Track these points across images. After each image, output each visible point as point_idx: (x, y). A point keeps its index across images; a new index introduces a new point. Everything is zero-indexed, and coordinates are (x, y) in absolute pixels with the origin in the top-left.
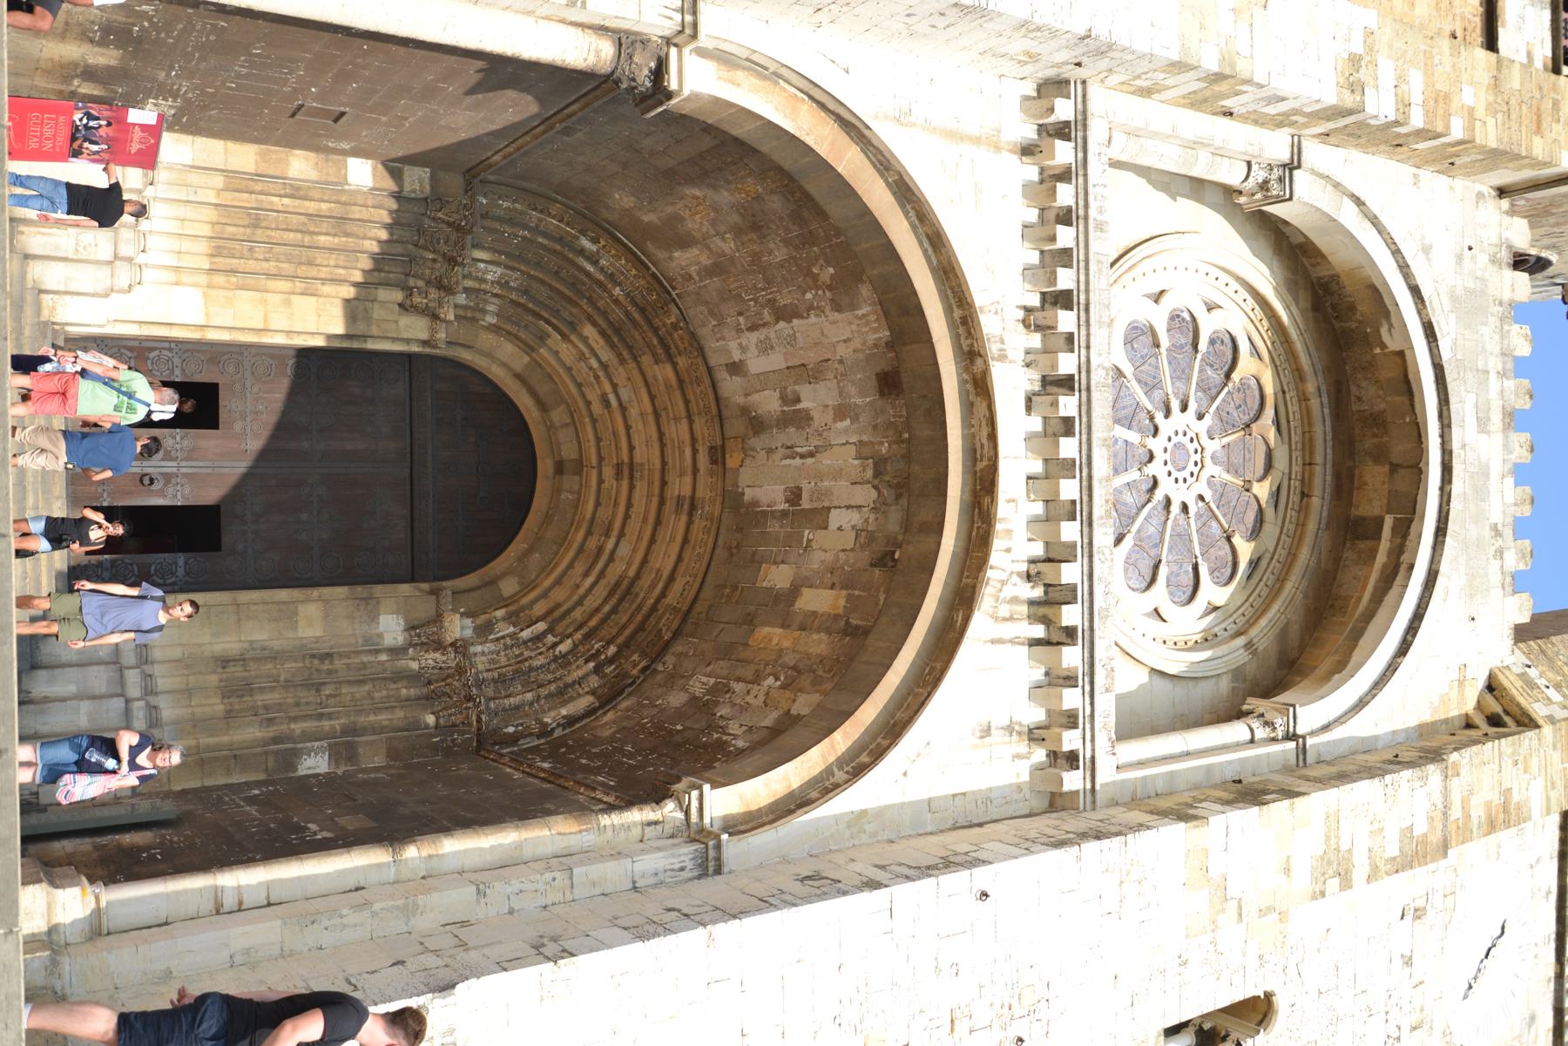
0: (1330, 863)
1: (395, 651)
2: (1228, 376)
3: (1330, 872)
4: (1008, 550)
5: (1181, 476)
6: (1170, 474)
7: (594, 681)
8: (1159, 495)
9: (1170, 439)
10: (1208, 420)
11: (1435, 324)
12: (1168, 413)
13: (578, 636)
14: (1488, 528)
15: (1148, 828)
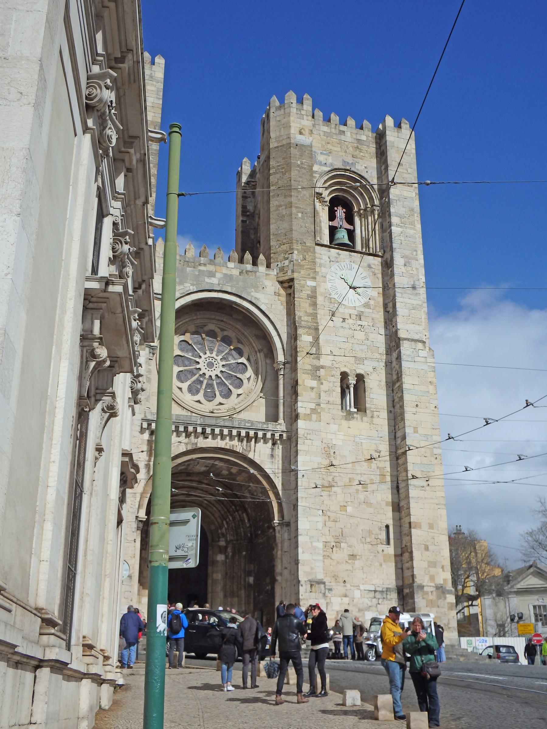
0: (313, 374)
1: (227, 557)
2: (190, 345)
3: (315, 373)
4: (236, 446)
5: (215, 366)
6: (214, 370)
7: (240, 512)
8: (220, 375)
9: (206, 369)
10: (201, 354)
11: (187, 293)
12: (200, 369)
13: (228, 514)
14: (240, 277)
15: (297, 429)
